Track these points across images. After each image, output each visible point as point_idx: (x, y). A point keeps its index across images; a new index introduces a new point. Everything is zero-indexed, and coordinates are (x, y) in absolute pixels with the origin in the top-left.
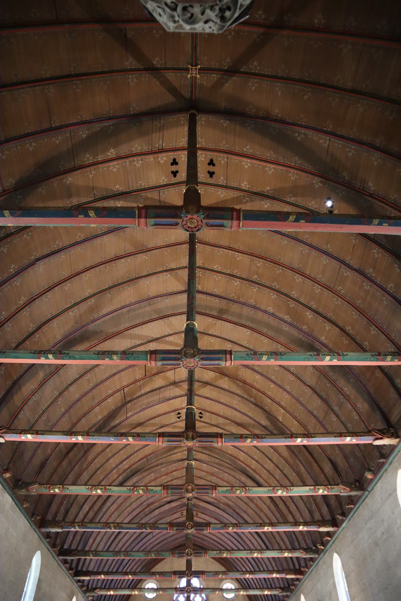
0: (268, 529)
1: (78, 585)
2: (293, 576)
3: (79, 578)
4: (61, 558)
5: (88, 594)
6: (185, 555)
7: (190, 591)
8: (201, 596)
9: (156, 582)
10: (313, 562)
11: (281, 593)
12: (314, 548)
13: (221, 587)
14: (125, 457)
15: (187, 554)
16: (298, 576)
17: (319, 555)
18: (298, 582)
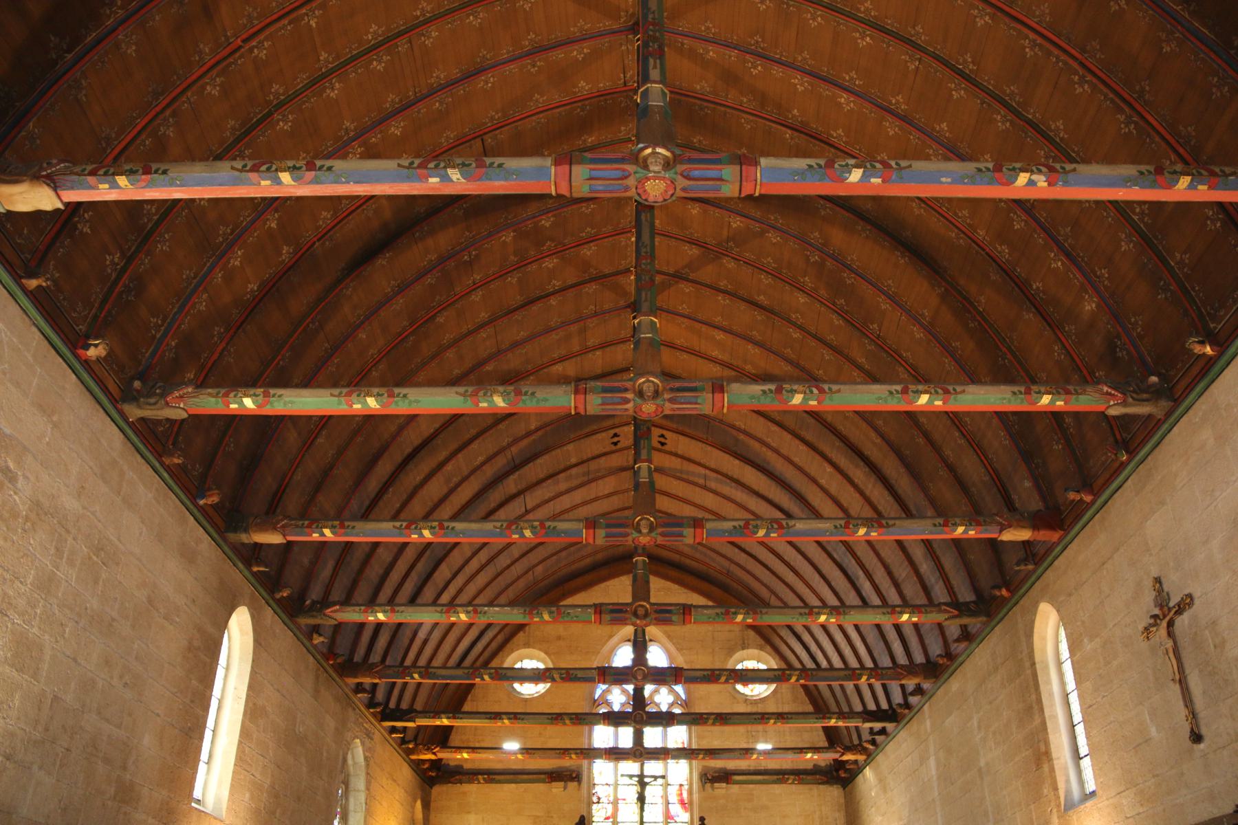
0: (1031, 183)
1: (254, 574)
2: (1024, 535)
3: (244, 538)
4: (135, 412)
5: (305, 621)
6: (630, 396)
7: (646, 615)
8: (672, 691)
9: (543, 655)
10: (1132, 453)
11: (956, 617)
12: (1154, 379)
13: (729, 666)
14: (391, 99)
15: (640, 394)
16: (1045, 536)
17: (1177, 402)
18: (1030, 567)
